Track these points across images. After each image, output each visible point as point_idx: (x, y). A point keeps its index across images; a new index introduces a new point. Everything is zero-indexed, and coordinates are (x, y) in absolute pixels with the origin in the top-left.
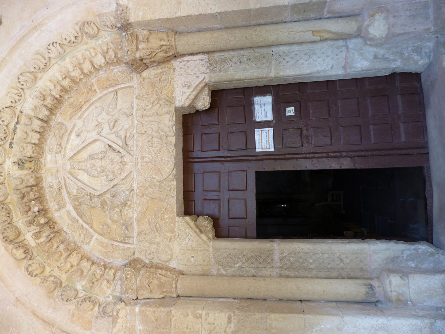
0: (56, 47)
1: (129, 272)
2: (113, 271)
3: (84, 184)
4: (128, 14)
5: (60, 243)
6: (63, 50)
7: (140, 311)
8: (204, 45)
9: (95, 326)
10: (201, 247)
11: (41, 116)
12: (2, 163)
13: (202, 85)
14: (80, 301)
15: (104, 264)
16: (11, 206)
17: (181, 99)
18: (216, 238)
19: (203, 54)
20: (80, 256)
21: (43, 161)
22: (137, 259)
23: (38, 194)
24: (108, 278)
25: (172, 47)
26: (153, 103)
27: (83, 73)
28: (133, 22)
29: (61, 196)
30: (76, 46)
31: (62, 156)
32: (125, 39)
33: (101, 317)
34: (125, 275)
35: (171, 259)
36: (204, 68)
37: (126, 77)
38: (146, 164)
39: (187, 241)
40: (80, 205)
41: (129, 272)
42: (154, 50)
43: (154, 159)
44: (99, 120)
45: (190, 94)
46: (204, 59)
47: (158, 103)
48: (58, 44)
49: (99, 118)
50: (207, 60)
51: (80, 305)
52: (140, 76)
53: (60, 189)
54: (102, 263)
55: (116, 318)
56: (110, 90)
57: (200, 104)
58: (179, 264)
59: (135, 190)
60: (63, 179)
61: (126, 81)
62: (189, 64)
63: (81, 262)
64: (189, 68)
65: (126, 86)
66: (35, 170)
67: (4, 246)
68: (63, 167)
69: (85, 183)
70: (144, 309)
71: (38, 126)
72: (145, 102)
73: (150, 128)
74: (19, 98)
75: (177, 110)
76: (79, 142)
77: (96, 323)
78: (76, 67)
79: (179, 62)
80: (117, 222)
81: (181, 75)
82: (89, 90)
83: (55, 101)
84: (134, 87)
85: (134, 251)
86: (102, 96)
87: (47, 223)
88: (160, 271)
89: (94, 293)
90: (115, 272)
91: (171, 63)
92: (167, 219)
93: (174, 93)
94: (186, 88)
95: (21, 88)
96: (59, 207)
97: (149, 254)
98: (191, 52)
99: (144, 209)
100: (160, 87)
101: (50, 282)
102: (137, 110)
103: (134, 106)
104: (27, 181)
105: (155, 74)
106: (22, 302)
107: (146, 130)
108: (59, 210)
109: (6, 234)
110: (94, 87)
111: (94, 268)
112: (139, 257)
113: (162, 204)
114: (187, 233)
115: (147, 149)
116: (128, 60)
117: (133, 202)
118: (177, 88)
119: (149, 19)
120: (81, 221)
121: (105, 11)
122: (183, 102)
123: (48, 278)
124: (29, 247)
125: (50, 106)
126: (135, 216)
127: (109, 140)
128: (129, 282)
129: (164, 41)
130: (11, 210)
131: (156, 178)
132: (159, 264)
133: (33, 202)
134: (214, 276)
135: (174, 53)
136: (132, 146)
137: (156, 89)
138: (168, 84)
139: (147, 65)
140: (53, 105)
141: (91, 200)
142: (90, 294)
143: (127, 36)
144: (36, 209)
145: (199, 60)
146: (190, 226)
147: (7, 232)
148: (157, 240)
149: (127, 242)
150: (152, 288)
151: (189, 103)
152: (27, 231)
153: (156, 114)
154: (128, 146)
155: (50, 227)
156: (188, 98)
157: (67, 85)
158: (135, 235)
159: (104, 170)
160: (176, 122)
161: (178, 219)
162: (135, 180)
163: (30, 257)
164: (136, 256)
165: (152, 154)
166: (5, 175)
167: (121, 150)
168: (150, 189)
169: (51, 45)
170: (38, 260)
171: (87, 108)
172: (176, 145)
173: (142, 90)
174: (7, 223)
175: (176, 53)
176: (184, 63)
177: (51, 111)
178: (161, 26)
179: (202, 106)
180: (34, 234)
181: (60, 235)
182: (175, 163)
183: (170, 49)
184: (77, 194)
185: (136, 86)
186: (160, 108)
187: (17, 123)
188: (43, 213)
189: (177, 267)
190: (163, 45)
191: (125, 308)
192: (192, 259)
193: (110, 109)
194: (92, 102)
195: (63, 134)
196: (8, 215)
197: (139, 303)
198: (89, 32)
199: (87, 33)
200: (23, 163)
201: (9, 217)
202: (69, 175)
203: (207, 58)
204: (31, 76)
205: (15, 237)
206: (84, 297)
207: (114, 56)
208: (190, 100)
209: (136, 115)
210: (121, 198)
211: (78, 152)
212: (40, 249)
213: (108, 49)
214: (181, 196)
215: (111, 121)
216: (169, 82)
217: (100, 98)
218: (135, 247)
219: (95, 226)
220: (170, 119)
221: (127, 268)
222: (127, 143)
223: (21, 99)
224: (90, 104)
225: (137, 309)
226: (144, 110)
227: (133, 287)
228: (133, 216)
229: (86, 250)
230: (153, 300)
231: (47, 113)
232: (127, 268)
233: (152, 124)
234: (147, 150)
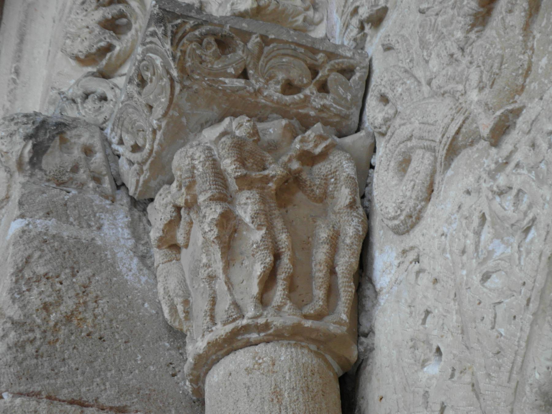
41: (158, 62)
221: (160, 31)
232: (160, 31)
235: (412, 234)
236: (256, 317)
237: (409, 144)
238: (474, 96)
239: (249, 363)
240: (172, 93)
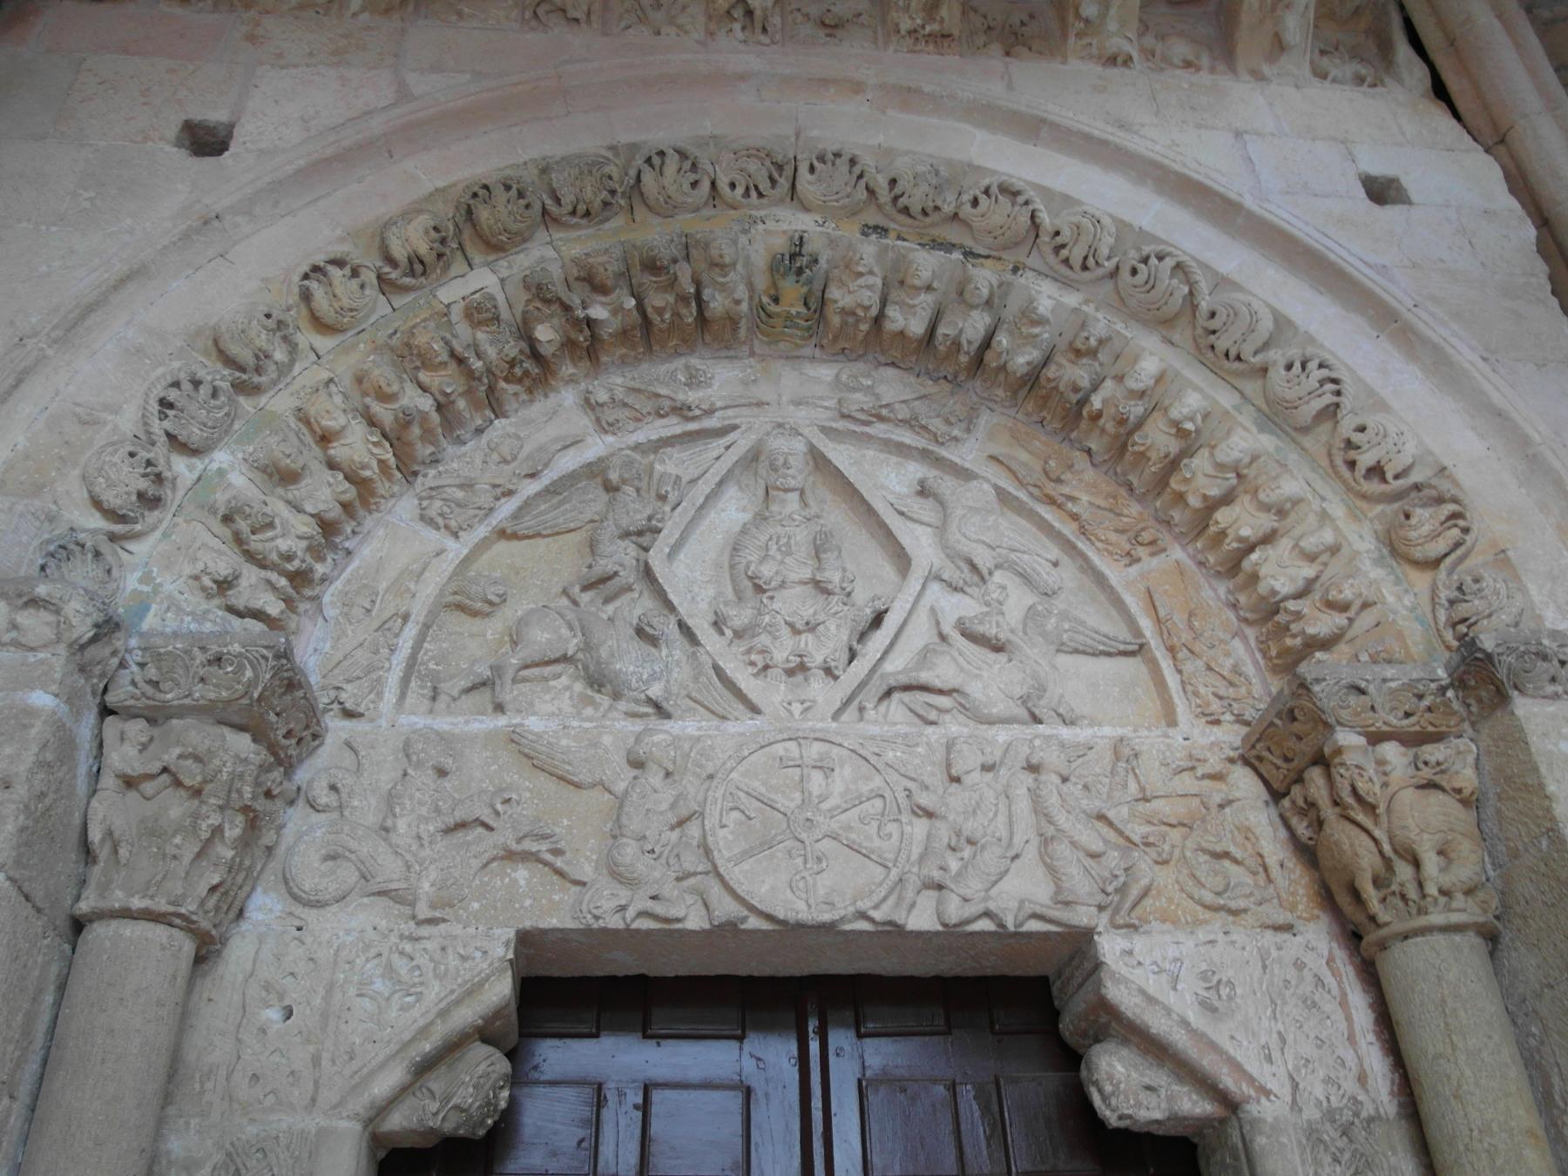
0: (1320, 392)
1: (249, 673)
2: (274, 608)
3: (702, 507)
4: (1550, 689)
5: (440, 398)
6: (1309, 420)
7: (31, 712)
8: (1459, 1086)
9: (10, 509)
10: (333, 1062)
11: (1003, 340)
12: (799, 199)
13: (1228, 1081)
15: (317, 576)
16: (617, 222)
17: (1140, 963)
18: (382, 1154)
19: (1395, 1089)
20: (367, 473)
21: (808, 351)
22: (318, 723)
23: (664, 326)
24: (244, 583)
25: (1414, 911)
26: (1102, 817)
27: (1212, 505)
28: (1513, 713)
29: (649, 413)
30: (1336, 473)
31: (827, 424)
32: (1415, 676)
33: (46, 536)
34: (240, 654)
35: (295, 898)
36: (1319, 1092)
37: (1216, 695)
38: (797, 778)
39: (379, 985)
40: (610, 488)
41: (249, 673)
42: (1384, 819)
43: (821, 819)
44: (999, 577)
45: (1168, 1011)
46: (1367, 1091)
47: (1106, 841)
48: (1335, 399)
50: (1368, 1110)
51: (132, 455)
52: (1231, 761)
53: (682, 411)
54: (320, 569)
55: (20, 596)
56: (1146, 624)
57: (1120, 1068)
58: (261, 940)
59: (668, 725)
60: (727, 422)
61: (1196, 694)
62: (1330, 1006)
63: (341, 476)
64: (1307, 1007)
65: (1171, 697)
66: (769, 316)
67: (450, 186)
69: (703, 512)
70: (33, 731)
71: (961, 331)
72: (1107, 780)
73: (978, 804)
74: (1076, 262)
75: (1080, 943)
76: (893, 492)
77: (22, 515)
78: (1233, 475)
79: (1330, 952)
80: (515, 643)
81: (1265, 967)
83: (1074, 398)
84: (1171, 732)
85: (362, 715)
86: (1111, 587)
87: (535, 355)
88: (233, 831)
89: (179, 520)
90: (268, 616)
91: (1316, 912)
92: (507, 880)
93: (1168, 926)
94: (1200, 992)
95: (1117, 268)
96: (601, 405)
97: (333, 788)
98: (1399, 1012)
99: (567, 767)
100: (1188, 854)
101: (265, 346)
102: (1062, 745)
103: (1077, 730)
104: (723, 284)
105: (1249, 829)
106: (194, 237)
107: (967, 780)
108: (589, 404)
109: (500, 196)
110: (1153, 554)
111: (304, 526)
112: (329, 739)
113: (587, 858)
114: (422, 984)
115: (872, 785)
116: (1316, 688)
117: (610, 715)
118: (1191, 944)
119: (1552, 788)
120: (532, 487)
121: (1533, 590)
122: (1124, 971)
123: (285, 338)
124: (434, 276)
125: (1051, 375)
126: (534, 723)
127: (910, 613)
128: (201, 672)
129: (1443, 870)
130: (602, 222)
131: (723, 826)
132: (278, 834)
133: (633, 302)
134: (158, 1134)
135: (1379, 926)
136: (885, 716)
137: (1175, 835)
138: (1208, 897)
139: (1296, 790)
140: (1056, 388)
141: (626, 535)
142: (177, 503)
144: (598, 312)
145: (1362, 1065)
146: (458, 1002)
147: (509, 201)
148: (402, 825)
149: (413, 684)
150: (148, 787)
151: (1123, 1008)
152: (504, 273)
153: (1049, 834)
154: (881, 699)
155: (514, 359)
156: (1151, 1000)
157: (1149, 442)
158: (443, 724)
159: (764, 591)
160: (1016, 934)
161: (504, 939)
162: (717, 728)
163: (393, 276)
164: (336, 727)
167: (861, 667)
168: (667, 796)
169: (1324, 373)
170: (373, 310)
171: (1051, 526)
172: (894, 931)
173: (1163, 769)
174: (548, 202)
175: (1384, 932)
176: (1329, 979)
177: (1025, 385)
178: (1515, 854)
179: (1111, 1078)
180: (492, 298)
181: (476, 405)
182: (800, 926)
183: (1401, 904)
184: (656, 476)
185: (1181, 740)
186: (1081, 855)
187: (968, 254)
188: (581, 339)
189: (244, 926)
190: (1416, 863)
191: (59, 640)
192: (274, 1014)
193: (1053, 620)
194: (1080, 545)
195: (924, 428)
196: (581, 208)
197: (77, 714)
198: (1413, 521)
199: (1407, 517)
200: (800, 271)
201: (573, 213)
202: (743, 443)
203: (1377, 1109)
204: (1177, 301)
205: (485, 227)
206: (166, 474)
207: (1313, 637)
208: (1138, 1011)
209: (1036, 736)
210: (629, 661)
211: (850, 484)
212: (422, 317)
213: (1343, 607)
214: (625, 963)
215: (997, 623)
216: (1222, 902)
217: (1100, 580)
219: (502, 546)
220: (1030, 902)
221: (272, 663)
222: (896, 696)
223: (1071, 268)
224: (1073, 538)
225: (42, 699)
226: (1065, 773)
227: (171, 690)
228: (534, 714)
229: (394, 505)
230: (82, 786)
231: (1022, 360)
232: (272, 663)
233: (996, 815)
234: (865, 789)
235: (306, 910)
236: (192, 913)
237: (347, 854)
238: (426, 886)
239: (164, 940)
240: (237, 699)
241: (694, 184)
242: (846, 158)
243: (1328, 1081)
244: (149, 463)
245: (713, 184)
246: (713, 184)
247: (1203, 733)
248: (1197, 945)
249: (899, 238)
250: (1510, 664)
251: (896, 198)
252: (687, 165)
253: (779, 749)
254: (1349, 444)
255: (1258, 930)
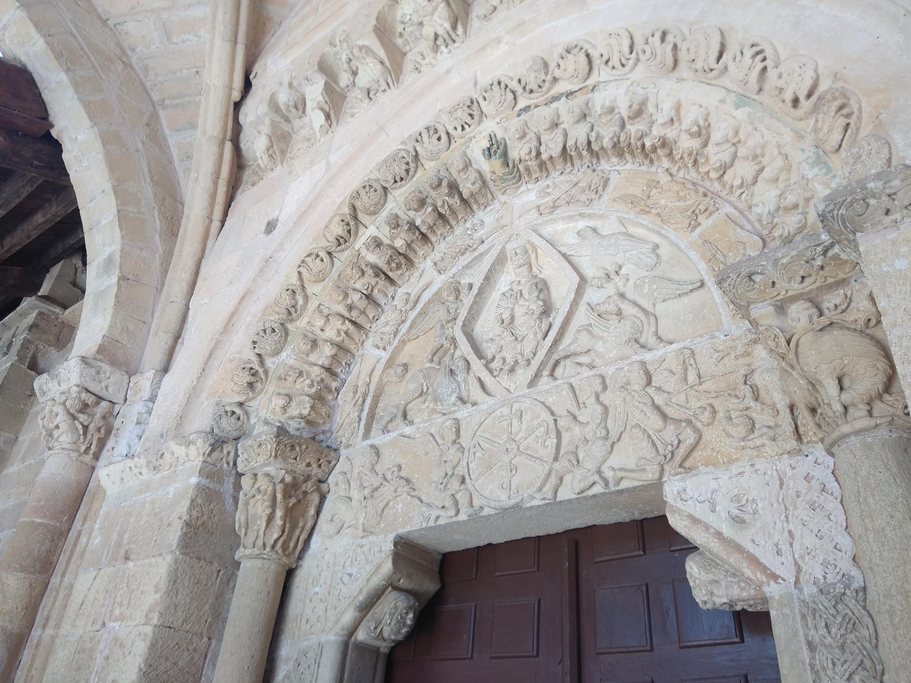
0: (753, 65)
14: (252, 365)
16: (420, 173)
21: (523, 188)
45: (707, 527)
49: (629, 266)
68: (513, 235)
81: (782, 484)
82: (691, 210)
93: (711, 468)
103: (656, 352)
104: (466, 179)
109: (363, 192)
110: (707, 217)
120: (412, 315)
122: (679, 504)
143: (819, 249)
152: (377, 224)
156: (694, 520)
157: (681, 150)
160: (620, 492)
164: (343, 452)
165: (526, 438)
166: (467, 133)
167: (541, 355)
176: (833, 485)
185: (722, 337)
193: (647, 286)
194: (663, 232)
201: (396, 182)
202: (494, 253)
206: (260, 370)
213: (796, 206)
218: (357, 447)
222: (562, 363)
224: (659, 230)
241: (439, 139)
242: (496, 83)
243: (825, 564)
244: (252, 369)
245: (448, 133)
246: (448, 133)
247: (738, 328)
248: (730, 478)
249: (536, 107)
250: (842, 215)
251: (524, 88)
252: (431, 132)
253: (498, 413)
254: (781, 90)
255: (777, 457)
